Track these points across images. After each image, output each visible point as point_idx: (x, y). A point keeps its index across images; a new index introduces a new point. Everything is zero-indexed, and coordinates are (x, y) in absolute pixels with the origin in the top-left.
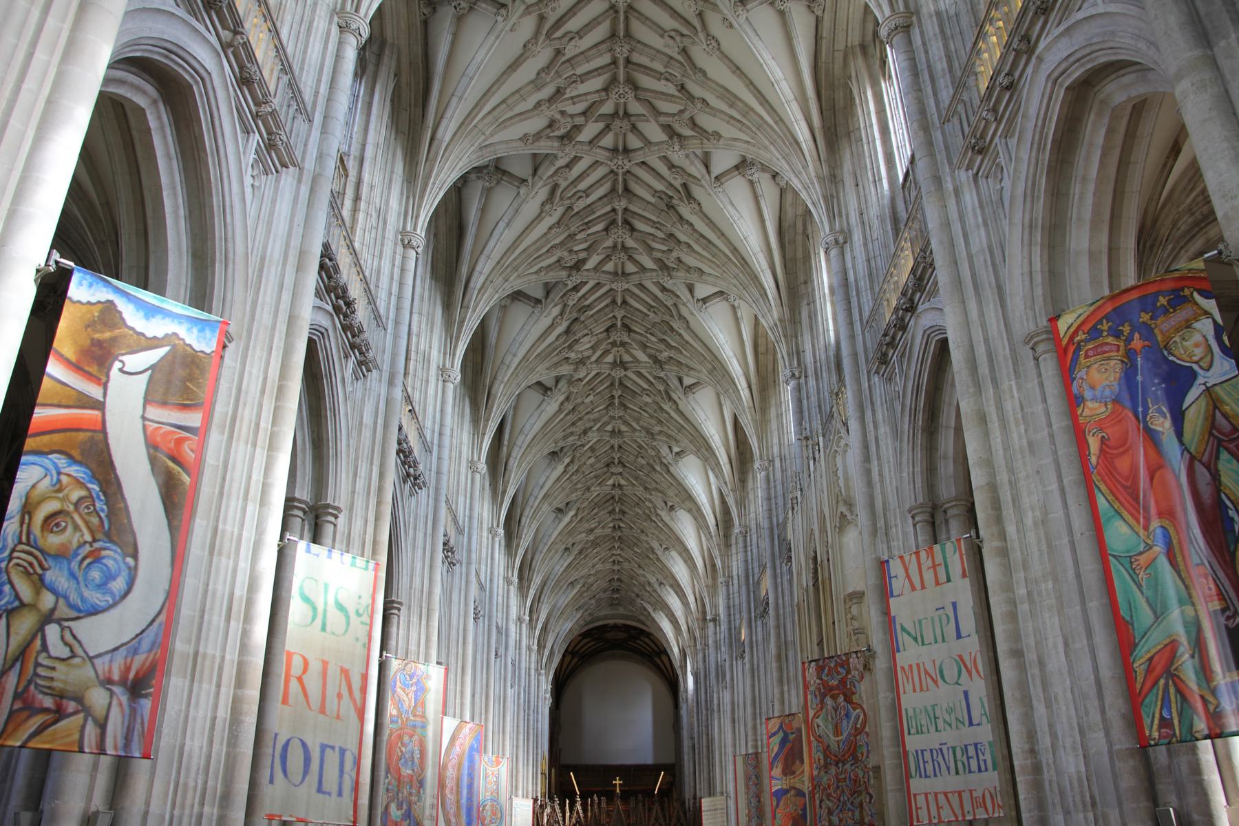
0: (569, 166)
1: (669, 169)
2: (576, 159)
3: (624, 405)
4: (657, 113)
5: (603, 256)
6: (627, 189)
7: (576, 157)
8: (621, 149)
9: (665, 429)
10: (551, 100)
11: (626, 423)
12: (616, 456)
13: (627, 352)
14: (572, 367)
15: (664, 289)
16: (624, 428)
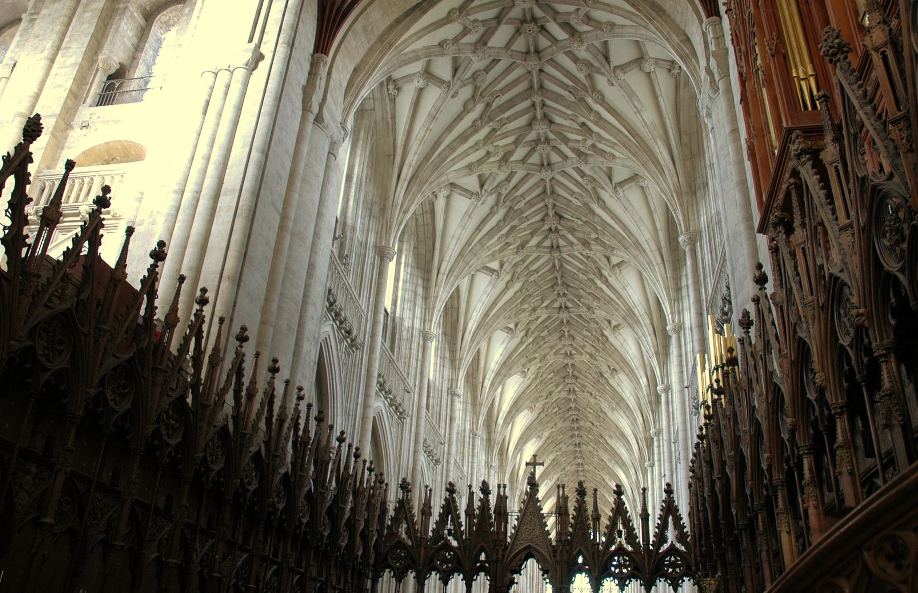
0: (508, 179)
1: (582, 177)
2: (512, 174)
3: (572, 336)
4: (566, 140)
5: (543, 236)
6: (553, 192)
7: (512, 172)
8: (545, 163)
9: (601, 355)
10: (487, 139)
11: (575, 349)
12: (570, 370)
13: (568, 300)
14: (528, 314)
15: (588, 257)
16: (574, 352)
